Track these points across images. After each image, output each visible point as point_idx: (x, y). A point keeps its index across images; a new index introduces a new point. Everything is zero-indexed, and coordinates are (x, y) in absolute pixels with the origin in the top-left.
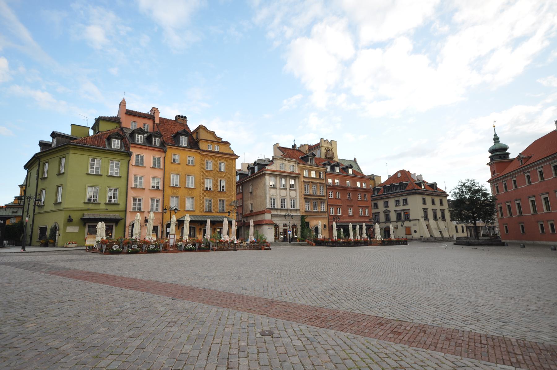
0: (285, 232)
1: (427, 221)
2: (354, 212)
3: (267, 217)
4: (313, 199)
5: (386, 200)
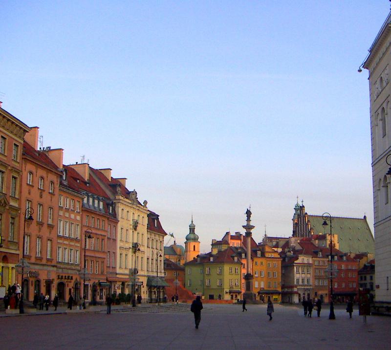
0: (304, 297)
3: (295, 289)
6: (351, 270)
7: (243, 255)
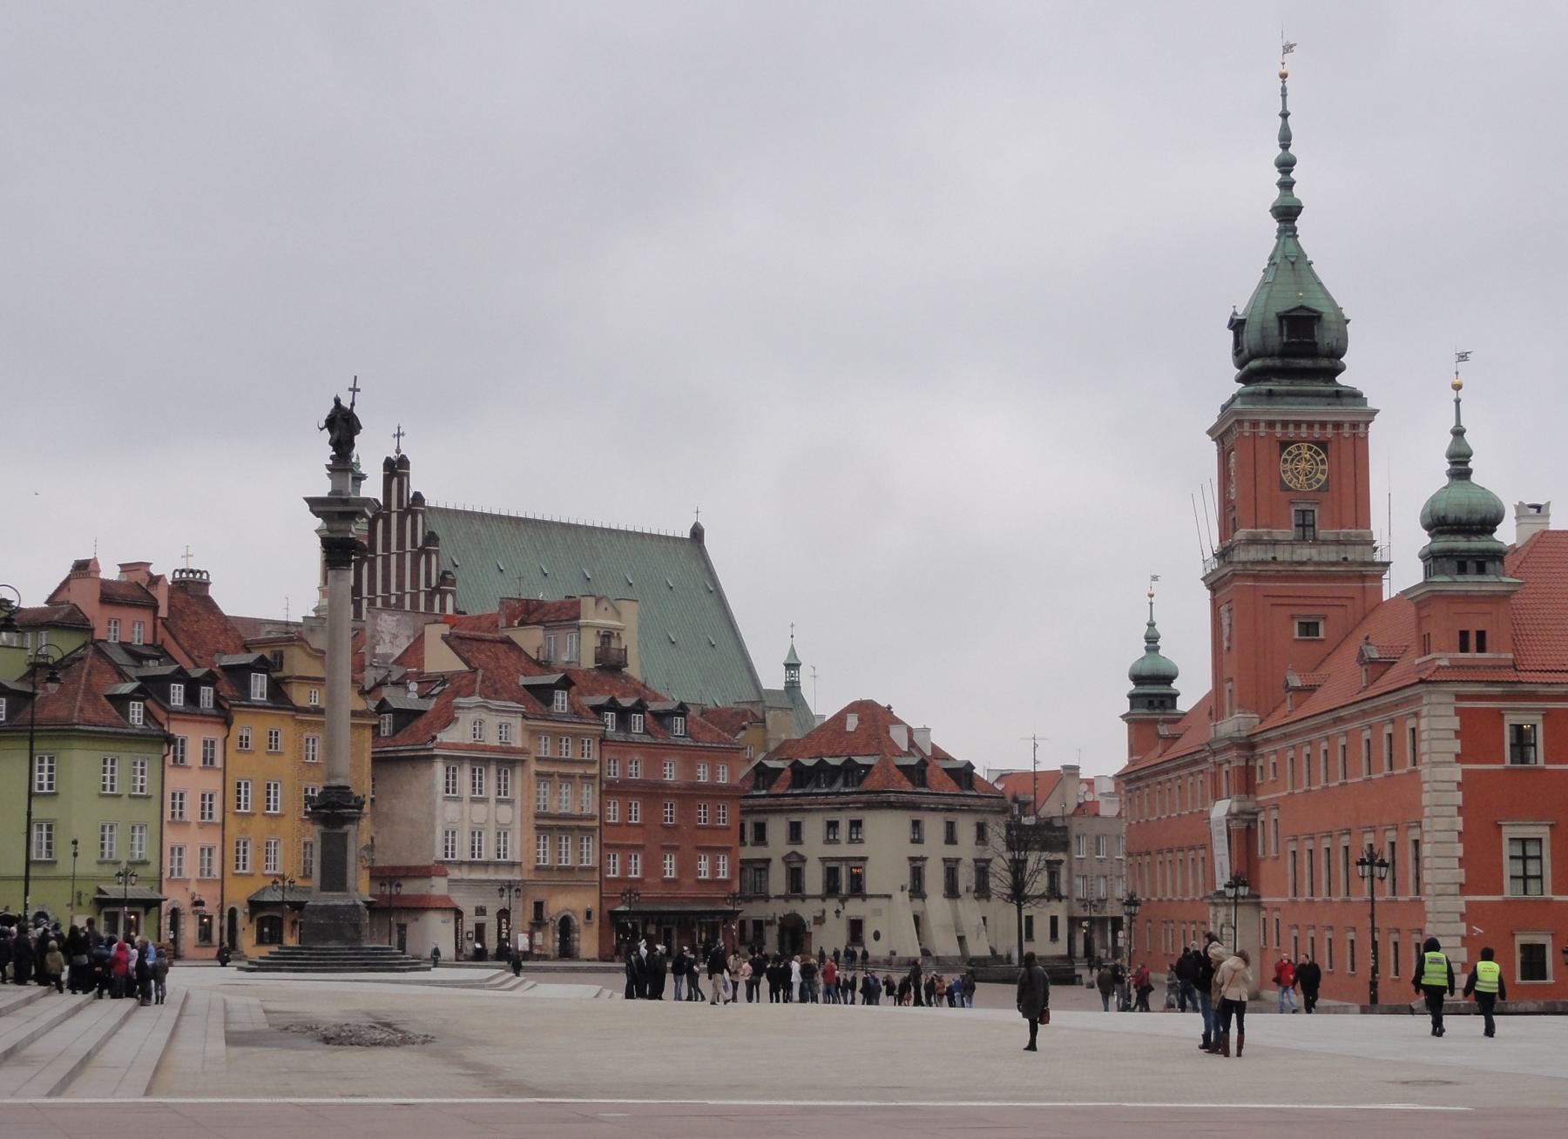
0: (480, 930)
1: (918, 902)
2: (680, 870)
3: (438, 886)
4: (561, 828)
5: (795, 818)
6: (713, 793)
7: (177, 694)
